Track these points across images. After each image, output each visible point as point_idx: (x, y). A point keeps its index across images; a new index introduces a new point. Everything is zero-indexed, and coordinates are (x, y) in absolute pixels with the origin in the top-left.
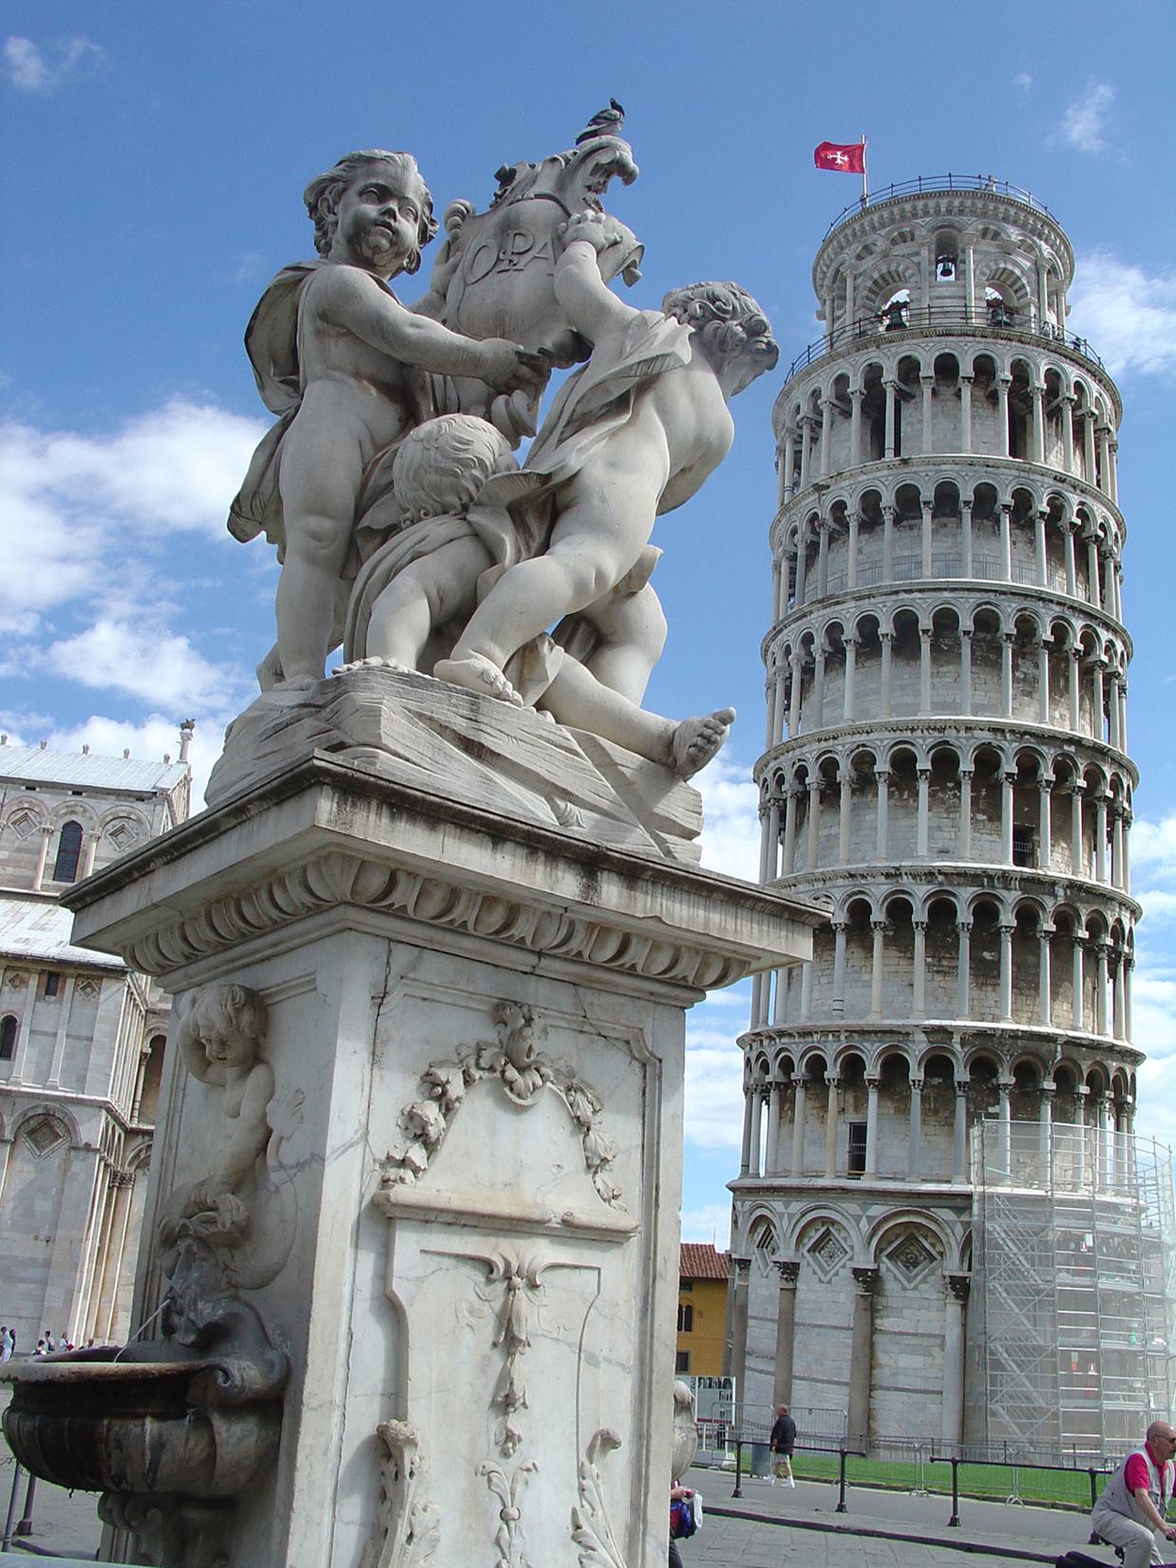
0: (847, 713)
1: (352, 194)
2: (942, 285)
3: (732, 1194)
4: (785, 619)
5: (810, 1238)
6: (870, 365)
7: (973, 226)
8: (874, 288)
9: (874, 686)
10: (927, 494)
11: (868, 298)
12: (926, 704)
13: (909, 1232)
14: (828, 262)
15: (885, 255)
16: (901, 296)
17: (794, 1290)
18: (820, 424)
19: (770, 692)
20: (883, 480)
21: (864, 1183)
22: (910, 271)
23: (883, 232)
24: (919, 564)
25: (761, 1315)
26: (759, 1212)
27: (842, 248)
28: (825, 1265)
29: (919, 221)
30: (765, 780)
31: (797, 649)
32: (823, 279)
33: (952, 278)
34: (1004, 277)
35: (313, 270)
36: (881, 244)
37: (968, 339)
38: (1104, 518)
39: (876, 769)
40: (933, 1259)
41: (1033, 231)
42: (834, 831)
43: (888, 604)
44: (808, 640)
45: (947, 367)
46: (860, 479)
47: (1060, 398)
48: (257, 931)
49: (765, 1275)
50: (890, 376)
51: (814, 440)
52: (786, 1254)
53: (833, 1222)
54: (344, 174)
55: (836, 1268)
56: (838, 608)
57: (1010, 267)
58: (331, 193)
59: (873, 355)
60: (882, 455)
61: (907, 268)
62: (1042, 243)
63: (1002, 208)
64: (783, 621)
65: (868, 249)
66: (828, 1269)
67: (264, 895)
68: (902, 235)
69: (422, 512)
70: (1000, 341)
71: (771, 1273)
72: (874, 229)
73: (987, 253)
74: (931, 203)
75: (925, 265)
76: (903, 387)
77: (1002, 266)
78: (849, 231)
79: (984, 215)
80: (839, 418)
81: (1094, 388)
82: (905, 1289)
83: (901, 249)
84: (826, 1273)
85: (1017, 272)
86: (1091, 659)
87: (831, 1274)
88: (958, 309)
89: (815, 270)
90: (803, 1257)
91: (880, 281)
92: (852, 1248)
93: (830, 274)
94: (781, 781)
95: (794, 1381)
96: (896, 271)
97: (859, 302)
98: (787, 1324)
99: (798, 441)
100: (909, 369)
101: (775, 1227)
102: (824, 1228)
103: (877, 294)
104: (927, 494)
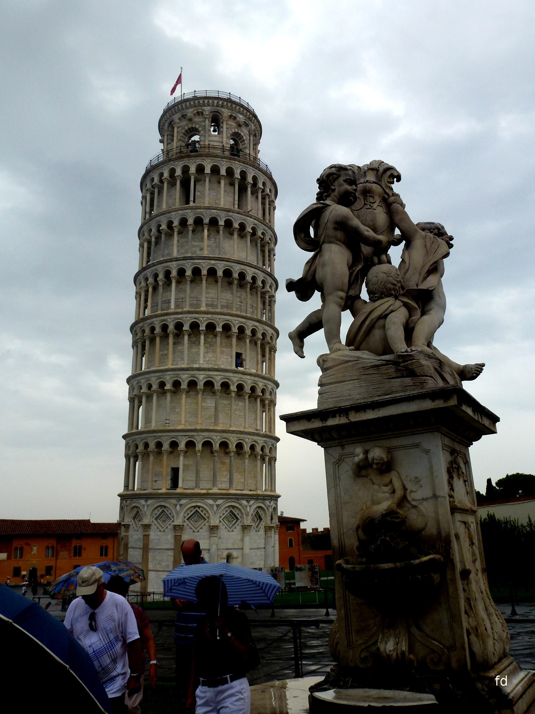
0: (173, 306)
1: (341, 180)
3: (120, 498)
4: (146, 267)
5: (156, 514)
6: (185, 165)
7: (226, 112)
8: (185, 133)
9: (182, 296)
10: (206, 221)
11: (183, 137)
12: (204, 305)
13: (195, 510)
14: (166, 119)
15: (190, 120)
16: (196, 138)
17: (148, 536)
18: (162, 188)
19: (138, 296)
20: (189, 213)
21: (178, 491)
23: (191, 110)
24: (202, 249)
26: (133, 505)
27: (173, 114)
29: (205, 108)
31: (151, 280)
32: (163, 126)
33: (216, 133)
34: (237, 135)
35: (330, 205)
37: (224, 160)
38: (271, 236)
39: (184, 329)
40: (205, 519)
41: (249, 118)
42: (165, 352)
44: (156, 276)
45: (215, 170)
47: (257, 187)
49: (136, 530)
50: (193, 170)
51: (160, 192)
52: (146, 521)
53: (165, 507)
54: (337, 173)
55: (167, 526)
56: (169, 264)
57: (239, 132)
58: (332, 178)
59: (185, 162)
60: (189, 204)
63: (238, 108)
65: (184, 116)
66: (163, 526)
68: (198, 113)
69: (383, 296)
70: (236, 162)
72: (187, 108)
73: (231, 125)
74: (211, 101)
75: (207, 126)
76: (197, 176)
77: (237, 131)
78: (176, 108)
80: (170, 186)
81: (269, 185)
82: (194, 532)
83: (197, 119)
84: (163, 528)
85: (242, 134)
86: (264, 290)
87: (165, 527)
88: (219, 147)
90: (153, 522)
91: (188, 131)
92: (173, 517)
93: (167, 124)
95: (149, 572)
97: (179, 138)
99: (152, 194)
100: (200, 169)
101: (141, 511)
102: (161, 510)
104: (206, 221)
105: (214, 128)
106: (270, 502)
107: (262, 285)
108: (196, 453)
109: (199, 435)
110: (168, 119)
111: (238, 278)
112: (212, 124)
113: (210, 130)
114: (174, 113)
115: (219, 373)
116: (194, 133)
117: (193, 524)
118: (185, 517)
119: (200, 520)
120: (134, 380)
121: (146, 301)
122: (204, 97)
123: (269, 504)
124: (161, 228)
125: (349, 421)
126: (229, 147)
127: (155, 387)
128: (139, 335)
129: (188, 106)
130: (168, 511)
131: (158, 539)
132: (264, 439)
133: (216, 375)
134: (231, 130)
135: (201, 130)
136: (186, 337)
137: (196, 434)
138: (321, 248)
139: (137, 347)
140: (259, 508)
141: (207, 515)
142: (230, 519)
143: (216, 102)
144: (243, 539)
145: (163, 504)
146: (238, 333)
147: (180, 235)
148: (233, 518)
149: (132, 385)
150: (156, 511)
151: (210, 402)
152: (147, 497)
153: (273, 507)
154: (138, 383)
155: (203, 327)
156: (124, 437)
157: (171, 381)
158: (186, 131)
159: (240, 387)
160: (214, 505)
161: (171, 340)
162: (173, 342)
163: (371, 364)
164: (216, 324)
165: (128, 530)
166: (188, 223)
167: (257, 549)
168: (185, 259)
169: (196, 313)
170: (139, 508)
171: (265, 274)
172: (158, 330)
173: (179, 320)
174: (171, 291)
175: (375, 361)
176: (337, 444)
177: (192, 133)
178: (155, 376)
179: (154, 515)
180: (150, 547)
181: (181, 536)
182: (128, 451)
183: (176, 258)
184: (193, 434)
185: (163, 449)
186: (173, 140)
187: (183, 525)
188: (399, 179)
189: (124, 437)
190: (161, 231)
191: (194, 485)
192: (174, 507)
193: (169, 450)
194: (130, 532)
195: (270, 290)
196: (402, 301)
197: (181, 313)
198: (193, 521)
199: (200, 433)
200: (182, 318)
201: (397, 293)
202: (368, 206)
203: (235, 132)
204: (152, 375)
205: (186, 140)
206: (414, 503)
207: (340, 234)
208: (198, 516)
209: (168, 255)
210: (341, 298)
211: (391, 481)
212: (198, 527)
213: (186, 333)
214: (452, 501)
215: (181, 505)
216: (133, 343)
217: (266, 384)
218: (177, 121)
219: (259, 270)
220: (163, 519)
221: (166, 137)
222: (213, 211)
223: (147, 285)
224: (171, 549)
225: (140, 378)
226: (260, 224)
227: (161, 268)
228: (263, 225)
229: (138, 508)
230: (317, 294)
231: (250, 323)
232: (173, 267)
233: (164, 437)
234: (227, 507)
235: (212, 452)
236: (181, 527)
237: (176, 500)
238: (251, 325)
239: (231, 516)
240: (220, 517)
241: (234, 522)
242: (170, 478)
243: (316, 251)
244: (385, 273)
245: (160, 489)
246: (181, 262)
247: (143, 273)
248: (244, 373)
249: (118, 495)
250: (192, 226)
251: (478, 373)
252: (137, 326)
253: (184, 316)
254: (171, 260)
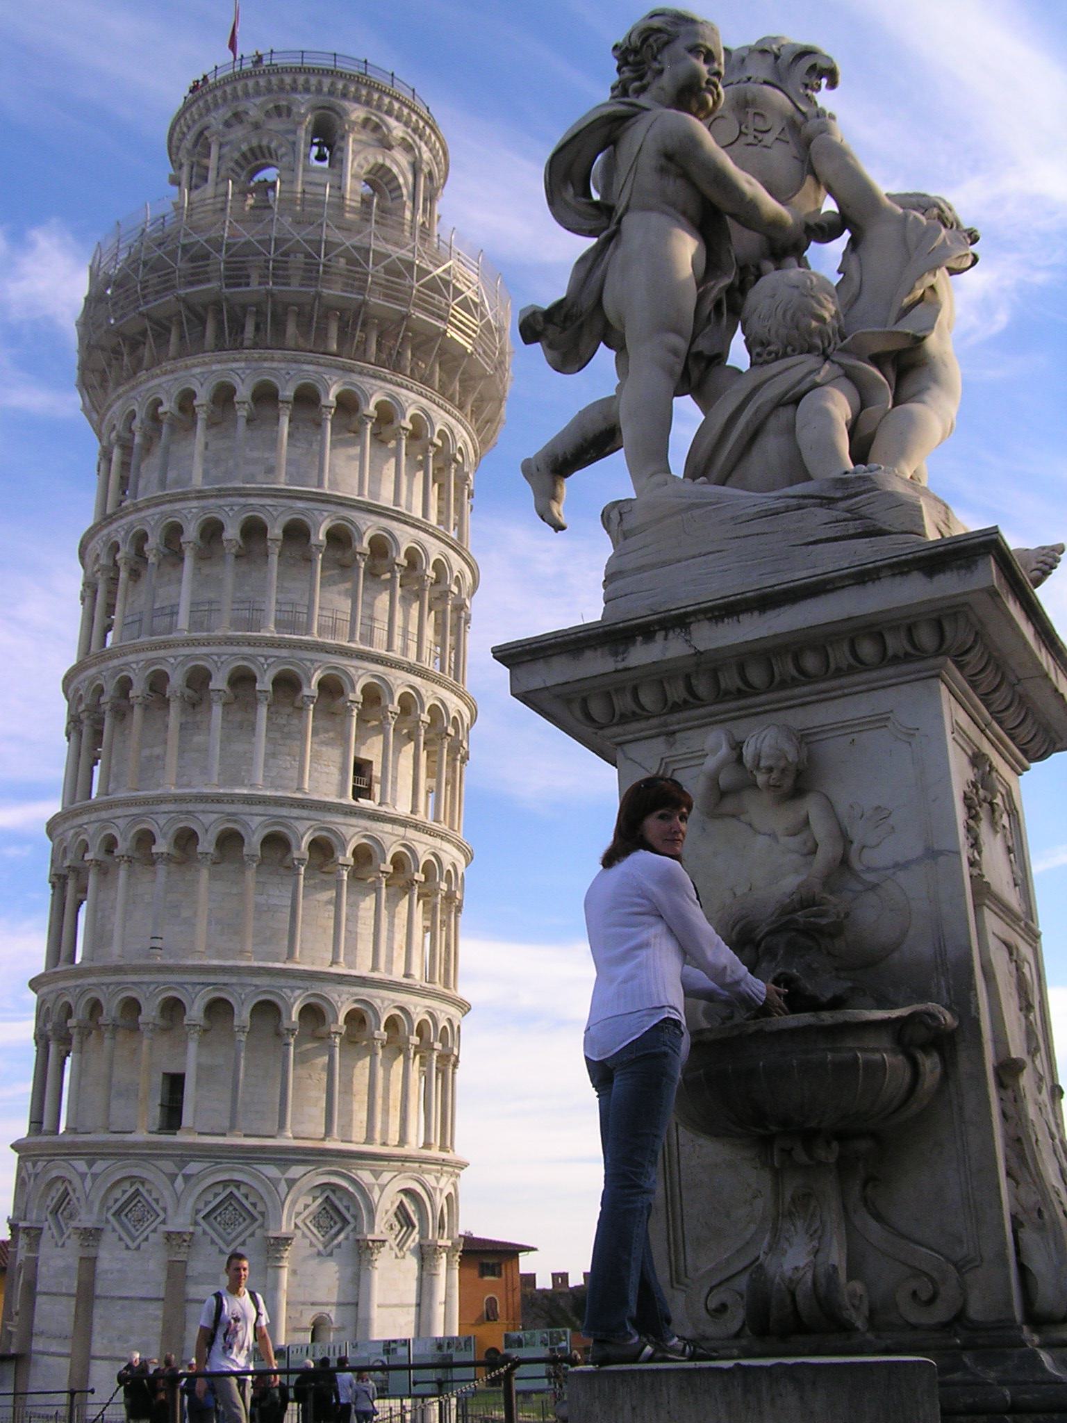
0: (183, 620)
2: (316, 170)
4: (114, 514)
5: (116, 1201)
8: (243, 163)
9: (212, 595)
10: (288, 392)
11: (233, 170)
13: (227, 1192)
15: (257, 126)
16: (270, 174)
17: (94, 1259)
19: (89, 592)
22: (283, 150)
23: (259, 101)
24: (271, 470)
25: (54, 1290)
26: (54, 1175)
27: (208, 110)
28: (133, 1230)
29: (298, 97)
30: (77, 690)
32: (181, 140)
33: (326, 164)
34: (379, 174)
35: (648, 110)
36: (254, 114)
39: (212, 685)
40: (254, 1219)
41: (415, 130)
42: (158, 750)
43: (236, 508)
44: (142, 538)
46: (214, 367)
48: (806, 677)
49: (60, 1244)
52: (87, 1220)
53: (143, 1182)
54: (669, 28)
55: (145, 1234)
56: (178, 506)
57: (388, 163)
58: (655, 41)
61: (280, 146)
62: (423, 144)
63: (387, 100)
64: (110, 516)
65: (238, 117)
67: (846, 648)
68: (277, 108)
69: (789, 349)
71: (69, 1242)
72: (247, 94)
74: (313, 81)
77: (380, 160)
79: (368, 103)
83: (275, 124)
84: (133, 1239)
85: (395, 170)
86: (440, 588)
87: (141, 1238)
89: (173, 129)
90: (107, 1221)
91: (249, 155)
92: (165, 1210)
93: (191, 137)
94: (100, 691)
95: (93, 1361)
96: (269, 148)
98: (86, 1296)
101: (74, 1190)
102: (132, 1190)
103: (242, 168)
105: (319, 151)
106: (437, 1179)
107: (434, 575)
108: (232, 1034)
109: (242, 985)
110: (194, 121)
111: (369, 553)
112: (316, 140)
113: (307, 156)
114: (212, 106)
115: (305, 813)
116: (263, 161)
117: (222, 1230)
118: (198, 1211)
119: (241, 1220)
120: (66, 826)
121: (110, 609)
122: (296, 68)
123: (434, 1184)
124: (161, 410)
125: (692, 651)
126: (359, 199)
127: (123, 847)
128: (88, 700)
129: (251, 91)
130: (149, 1192)
131: (118, 1271)
132: (428, 1002)
133: (297, 818)
134: (366, 159)
135: (282, 156)
136: (217, 710)
137: (234, 980)
138: (619, 222)
139: (80, 734)
140: (406, 1195)
141: (260, 1207)
142: (325, 1222)
143: (327, 83)
144: (359, 1280)
145: (136, 1172)
146: (363, 704)
147: (214, 431)
148: (332, 1219)
149: (62, 841)
150: (117, 1193)
151: (277, 893)
152: (93, 1154)
153: (445, 1194)
154: (77, 834)
155: (265, 683)
156: (35, 984)
157: (171, 833)
158: (244, 155)
159: (364, 856)
160: (280, 1179)
161: (174, 716)
162: (181, 724)
163: (756, 509)
164: (302, 676)
165: (38, 1245)
166: (236, 399)
167: (396, 1306)
168: (221, 493)
169: (251, 642)
170: (70, 1182)
171: (442, 545)
172: (137, 690)
173: (201, 663)
174: (180, 581)
175: (765, 500)
176: (653, 732)
177: (258, 162)
178: (126, 816)
179: (111, 1202)
180: (98, 1291)
181: (185, 1262)
182: (45, 1025)
183: (199, 491)
184: (226, 979)
185: (141, 1019)
186: (206, 179)
187: (192, 1234)
188: (831, 76)
189: (35, 984)
190: (161, 417)
191: (227, 1123)
192: (168, 1183)
193: (159, 1021)
194: (41, 1252)
195: (455, 589)
196: (840, 365)
197: (207, 643)
198: (220, 1224)
199: (248, 980)
200: (207, 655)
201: (829, 345)
202: (750, 139)
203: (376, 164)
204: (118, 812)
205: (242, 178)
206: (870, 877)
207: (674, 187)
208: (235, 1209)
209: (177, 483)
210: (675, 352)
211: (806, 822)
212: (237, 1237)
213: (215, 698)
214: (975, 874)
215: (187, 1178)
216: (68, 723)
217: (435, 848)
218: (221, 127)
219: (426, 531)
220: (136, 1214)
221: (186, 169)
222: (306, 367)
223: (115, 562)
224: (158, 1299)
225: (85, 819)
226: (435, 407)
227: (157, 517)
228: (442, 413)
229: (66, 1184)
230: (605, 356)
231: (396, 678)
232: (189, 516)
233: (144, 987)
234: (317, 1186)
235: (278, 1034)
236: (187, 1238)
237: (173, 1161)
238: (399, 682)
239: (327, 1212)
240: (299, 1214)
241: (333, 1231)
242: (159, 1101)
243: (603, 235)
244: (798, 287)
245: (131, 1132)
246: (212, 501)
247: (105, 532)
248: (375, 817)
249: (12, 1146)
250: (246, 406)
251: (1046, 568)
252: (82, 676)
253: (214, 649)
254: (184, 497)
